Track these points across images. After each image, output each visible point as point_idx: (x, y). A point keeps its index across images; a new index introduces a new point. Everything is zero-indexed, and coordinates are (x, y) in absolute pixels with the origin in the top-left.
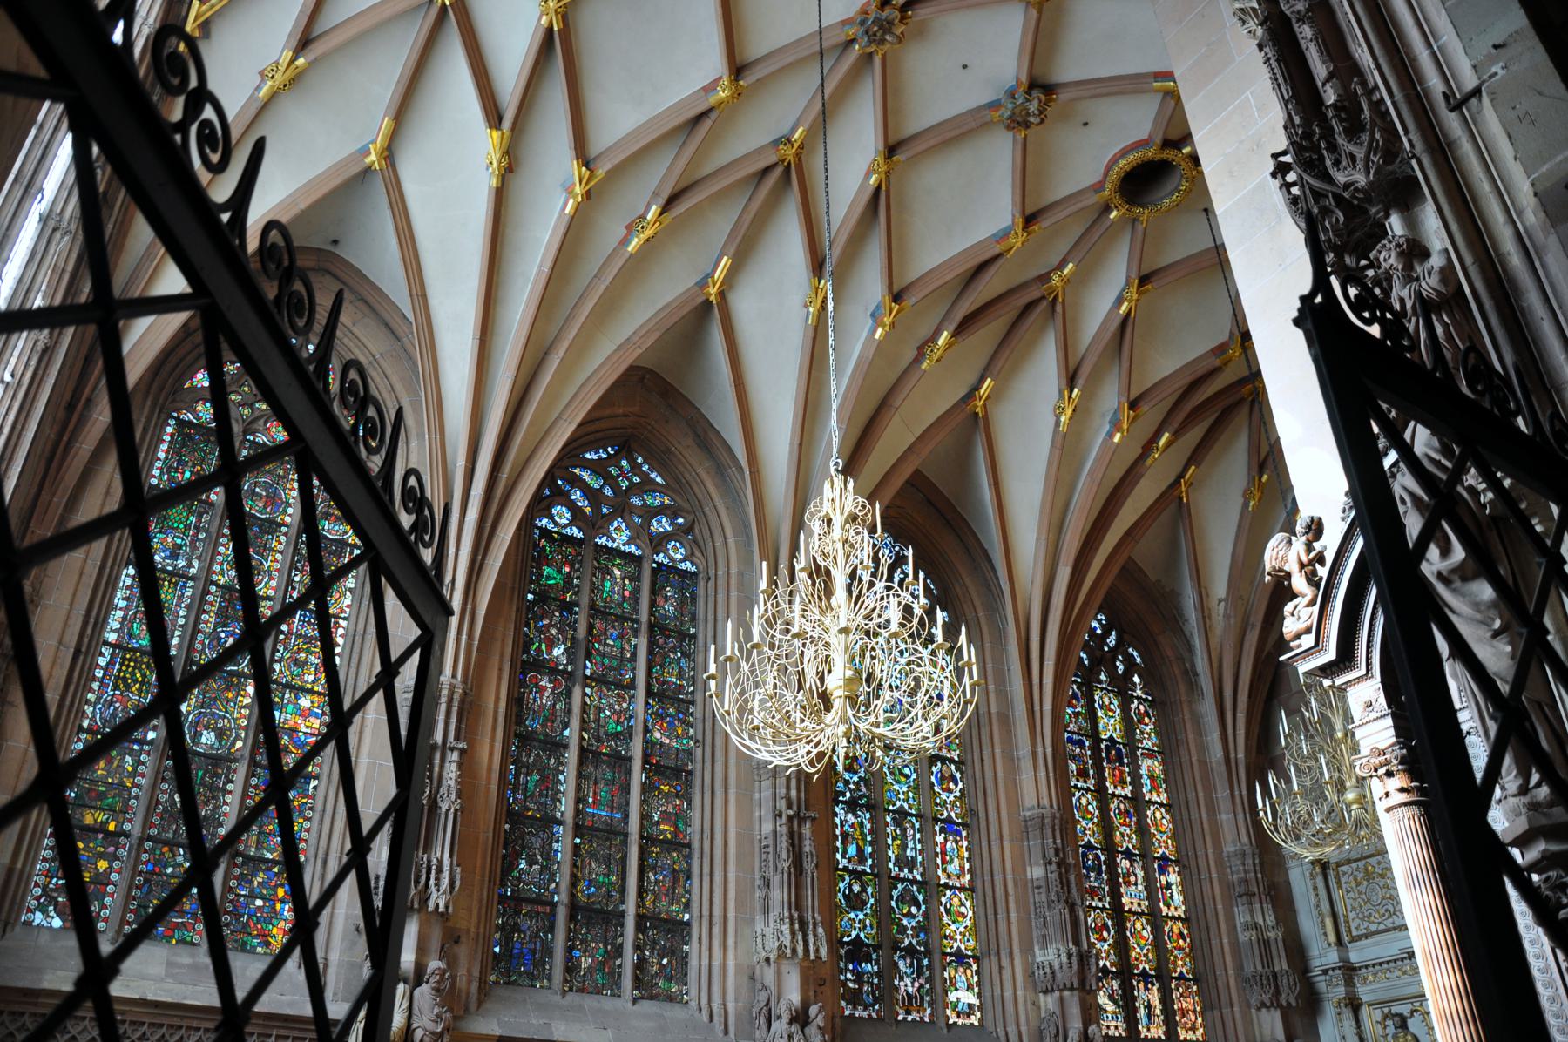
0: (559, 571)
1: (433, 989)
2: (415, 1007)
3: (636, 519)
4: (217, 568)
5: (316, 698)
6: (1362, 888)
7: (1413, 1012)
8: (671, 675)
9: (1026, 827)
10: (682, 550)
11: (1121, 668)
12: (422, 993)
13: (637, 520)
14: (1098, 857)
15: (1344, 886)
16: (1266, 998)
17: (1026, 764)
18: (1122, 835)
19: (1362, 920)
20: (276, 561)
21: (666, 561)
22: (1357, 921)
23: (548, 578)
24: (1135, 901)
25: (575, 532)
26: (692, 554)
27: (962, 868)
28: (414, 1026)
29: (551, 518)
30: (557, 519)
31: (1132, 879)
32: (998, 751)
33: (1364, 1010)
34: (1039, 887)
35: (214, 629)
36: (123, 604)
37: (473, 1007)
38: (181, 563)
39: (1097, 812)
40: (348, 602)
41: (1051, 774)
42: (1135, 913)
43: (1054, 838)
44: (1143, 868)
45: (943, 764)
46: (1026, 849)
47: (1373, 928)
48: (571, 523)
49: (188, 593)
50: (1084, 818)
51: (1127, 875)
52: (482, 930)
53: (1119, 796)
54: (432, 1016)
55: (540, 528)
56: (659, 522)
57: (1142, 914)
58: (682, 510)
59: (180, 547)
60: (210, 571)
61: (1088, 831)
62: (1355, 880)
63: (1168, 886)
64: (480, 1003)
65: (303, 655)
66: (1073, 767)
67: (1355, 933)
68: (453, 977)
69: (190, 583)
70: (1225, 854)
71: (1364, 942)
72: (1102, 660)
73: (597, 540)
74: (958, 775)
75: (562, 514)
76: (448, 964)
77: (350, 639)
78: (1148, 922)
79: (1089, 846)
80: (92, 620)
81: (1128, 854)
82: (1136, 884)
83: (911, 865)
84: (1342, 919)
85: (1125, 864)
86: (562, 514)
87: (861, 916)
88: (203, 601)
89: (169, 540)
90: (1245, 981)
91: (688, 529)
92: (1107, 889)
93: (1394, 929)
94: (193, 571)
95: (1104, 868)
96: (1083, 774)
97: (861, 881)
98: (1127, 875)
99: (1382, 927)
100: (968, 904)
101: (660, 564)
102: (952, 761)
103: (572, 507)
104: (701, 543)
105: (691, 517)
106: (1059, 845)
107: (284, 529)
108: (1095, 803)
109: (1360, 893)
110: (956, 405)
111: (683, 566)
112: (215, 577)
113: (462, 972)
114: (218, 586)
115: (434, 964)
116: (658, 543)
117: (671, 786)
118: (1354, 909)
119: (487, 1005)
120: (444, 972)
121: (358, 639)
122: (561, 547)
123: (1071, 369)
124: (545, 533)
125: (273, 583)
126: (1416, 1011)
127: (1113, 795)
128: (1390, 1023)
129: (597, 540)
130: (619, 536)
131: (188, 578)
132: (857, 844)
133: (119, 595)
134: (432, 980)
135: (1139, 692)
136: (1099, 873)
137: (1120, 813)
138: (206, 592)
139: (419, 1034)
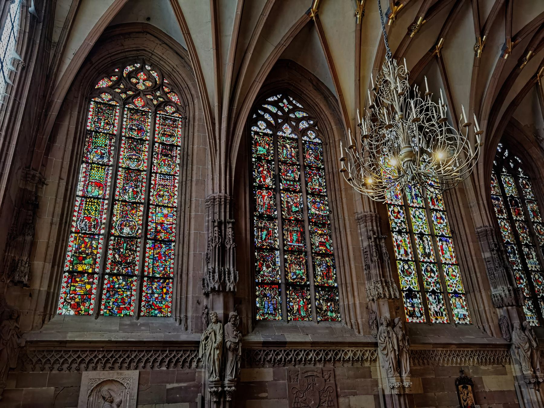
0: (264, 148)
1: (232, 324)
2: (226, 334)
3: (293, 123)
4: (121, 161)
5: (169, 209)
8: (315, 185)
9: (479, 236)
10: (314, 134)
11: (512, 165)
12: (228, 326)
13: (294, 124)
14: (512, 248)
17: (475, 209)
18: (523, 237)
20: (145, 155)
21: (308, 139)
23: (260, 151)
24: (534, 266)
25: (269, 131)
26: (318, 135)
27: (451, 256)
28: (226, 340)
29: (258, 126)
30: (260, 126)
31: (531, 256)
32: (461, 204)
34: (489, 261)
35: (123, 186)
36: (83, 179)
37: (250, 330)
38: (106, 160)
39: (509, 228)
40: (178, 169)
41: (488, 212)
42: (534, 271)
43: (493, 239)
44: (535, 251)
45: (437, 212)
46: (480, 245)
48: (266, 128)
49: (110, 172)
50: (504, 231)
51: (528, 255)
52: (250, 298)
53: (519, 221)
54: (234, 336)
55: (254, 131)
56: (303, 124)
57: (538, 271)
58: (312, 118)
59: (104, 154)
60: (118, 162)
61: (507, 235)
64: (253, 329)
65: (162, 193)
66: (496, 209)
68: (241, 319)
69: (111, 168)
72: (502, 162)
73: (278, 134)
74: (444, 216)
75: (262, 125)
76: (237, 313)
77: (181, 184)
78: (541, 275)
79: (508, 243)
80: (70, 187)
81: (527, 245)
82: (533, 258)
83: (428, 255)
85: (526, 250)
86: (262, 125)
87: (410, 279)
88: (116, 175)
89: (99, 151)
91: (315, 125)
92: (519, 261)
94: (111, 163)
95: (516, 252)
96: (500, 212)
97: (408, 264)
98: (528, 255)
100: (456, 271)
101: (305, 141)
102: (440, 211)
103: (266, 121)
104: (322, 130)
105: (316, 120)
106: (496, 243)
107: (147, 142)
108: (508, 224)
110: (427, 54)
111: (315, 141)
112: (120, 165)
113: (244, 315)
114: (123, 168)
115: (231, 313)
116: (304, 132)
117: (322, 231)
119: (256, 329)
120: (236, 316)
121: (184, 183)
122: (263, 138)
123: (482, 25)
124: (257, 133)
125: (146, 165)
127: (516, 220)
129: (278, 134)
130: (287, 131)
131: (109, 166)
132: (404, 249)
133: (80, 176)
134: (231, 320)
135: (522, 175)
136: (515, 254)
137: (520, 228)
138: (117, 171)
139: (228, 344)
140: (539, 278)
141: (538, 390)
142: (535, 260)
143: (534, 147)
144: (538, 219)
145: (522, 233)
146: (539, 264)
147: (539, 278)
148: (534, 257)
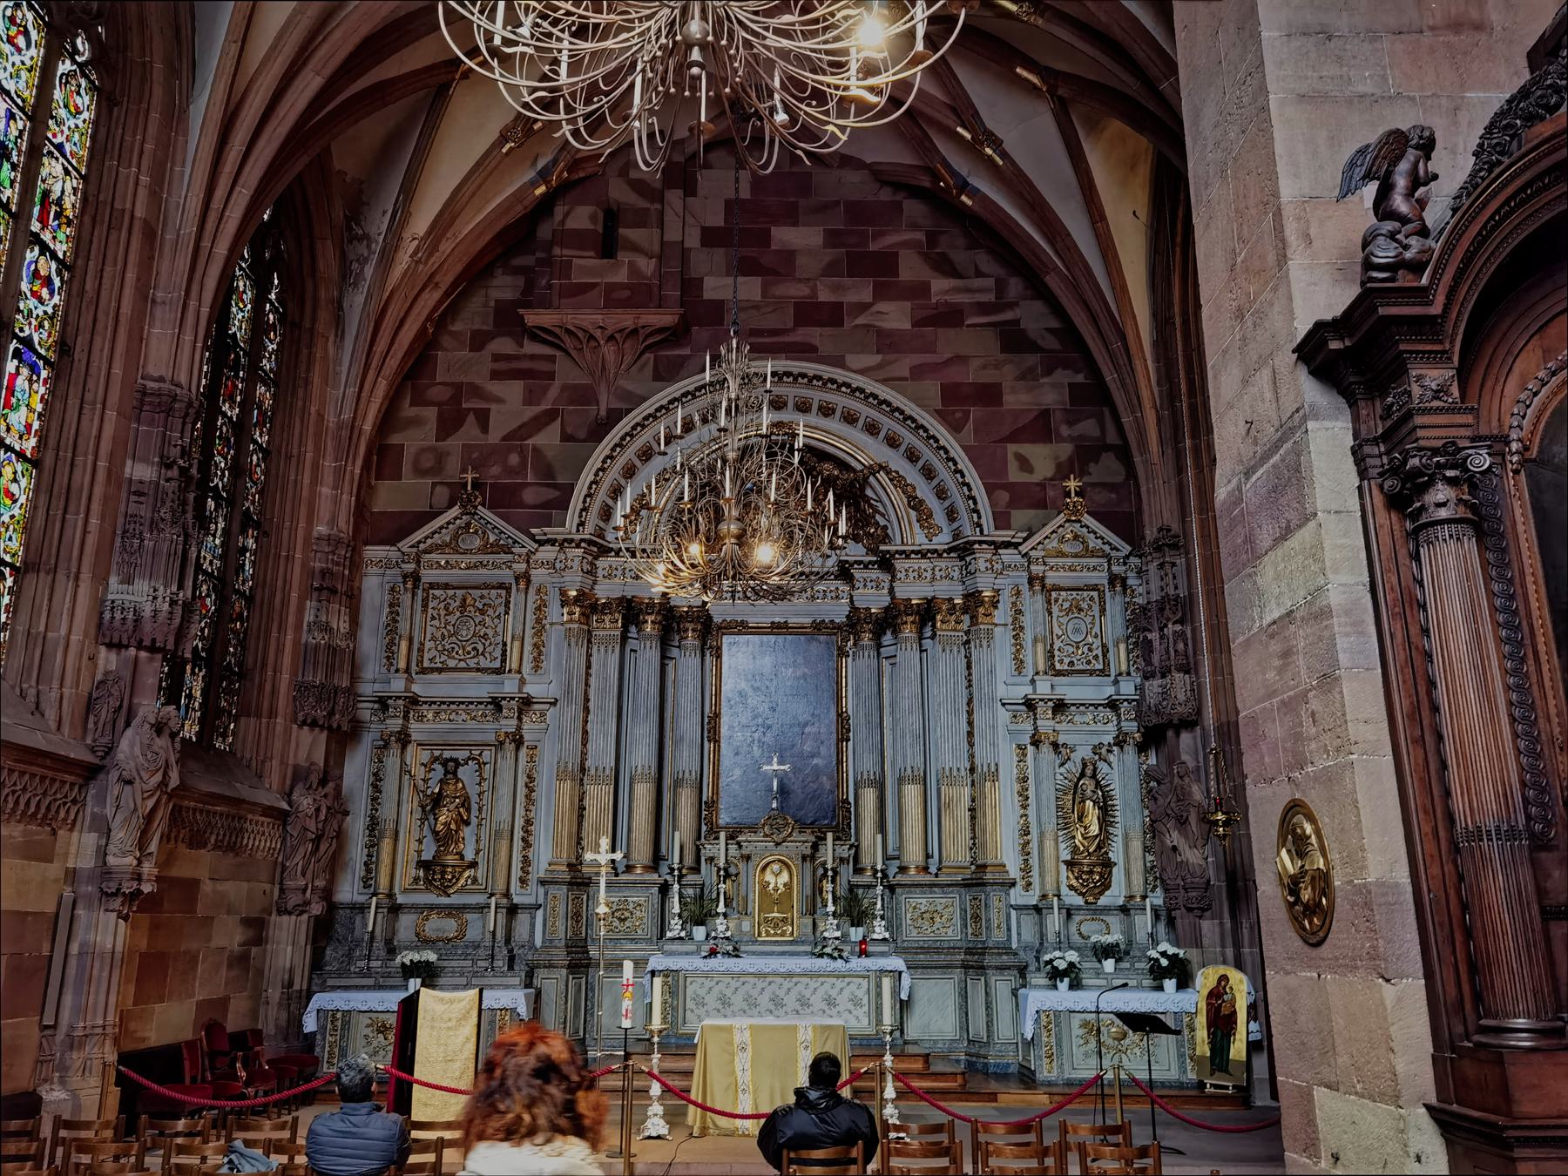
6: (453, 619)
7: (469, 759)
15: (430, 611)
16: (320, 714)
19: (441, 652)
22: (434, 652)
33: (410, 749)
47: (452, 663)
62: (446, 608)
63: (244, 550)
67: (426, 664)
70: (315, 534)
71: (435, 676)
84: (416, 646)
90: (301, 688)
93: (478, 670)
99: (462, 665)
109: (447, 623)
118: (433, 639)
126: (474, 759)
128: (437, 766)
140: (208, 595)
141: (126, 919)
142: (217, 541)
143: (329, 242)
144: (261, 436)
145: (219, 454)
146: (221, 558)
147: (208, 595)
148: (219, 533)
